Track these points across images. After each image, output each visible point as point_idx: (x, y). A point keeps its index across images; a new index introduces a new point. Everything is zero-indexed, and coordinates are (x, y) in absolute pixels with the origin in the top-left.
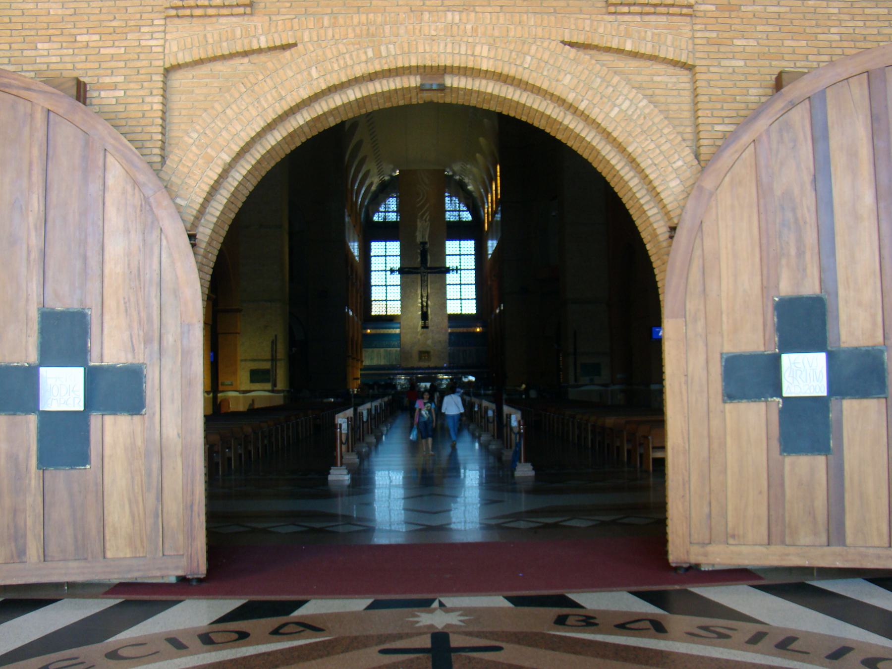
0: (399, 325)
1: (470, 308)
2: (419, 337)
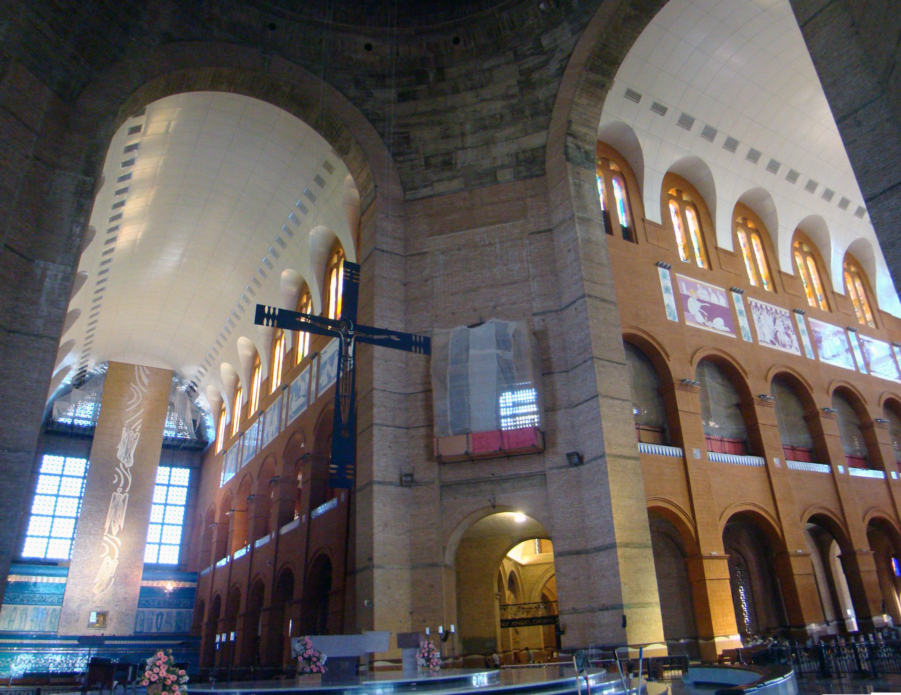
0: (65, 572)
1: (171, 556)
2: (96, 590)
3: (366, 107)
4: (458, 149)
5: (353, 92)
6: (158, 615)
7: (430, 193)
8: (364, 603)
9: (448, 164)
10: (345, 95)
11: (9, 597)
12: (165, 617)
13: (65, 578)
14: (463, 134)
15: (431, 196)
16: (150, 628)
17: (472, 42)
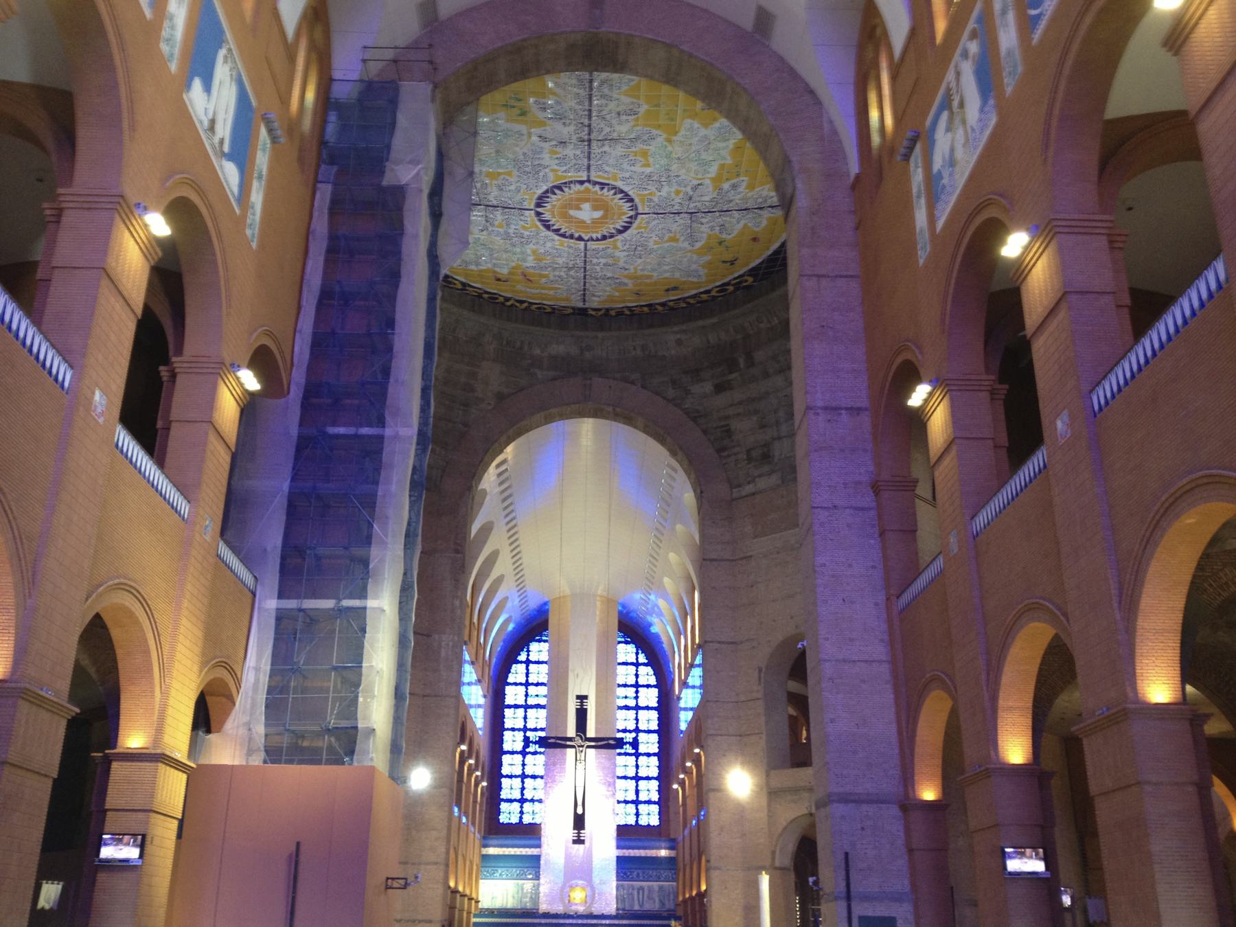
3: (686, 406)
4: (774, 439)
5: (671, 393)
6: (639, 890)
7: (753, 490)
8: (808, 882)
9: (766, 457)
10: (664, 398)
11: (488, 872)
12: (646, 893)
13: (538, 850)
14: (778, 423)
15: (754, 494)
16: (632, 905)
17: (775, 319)
